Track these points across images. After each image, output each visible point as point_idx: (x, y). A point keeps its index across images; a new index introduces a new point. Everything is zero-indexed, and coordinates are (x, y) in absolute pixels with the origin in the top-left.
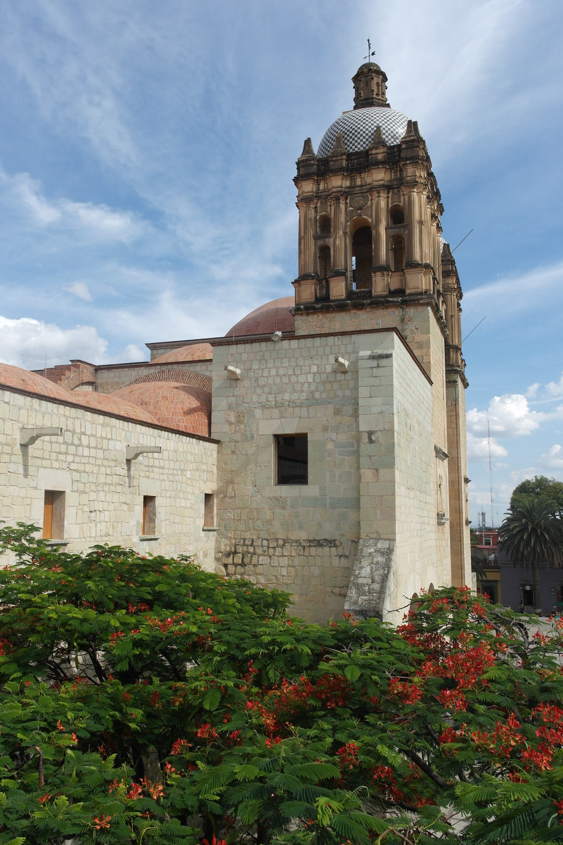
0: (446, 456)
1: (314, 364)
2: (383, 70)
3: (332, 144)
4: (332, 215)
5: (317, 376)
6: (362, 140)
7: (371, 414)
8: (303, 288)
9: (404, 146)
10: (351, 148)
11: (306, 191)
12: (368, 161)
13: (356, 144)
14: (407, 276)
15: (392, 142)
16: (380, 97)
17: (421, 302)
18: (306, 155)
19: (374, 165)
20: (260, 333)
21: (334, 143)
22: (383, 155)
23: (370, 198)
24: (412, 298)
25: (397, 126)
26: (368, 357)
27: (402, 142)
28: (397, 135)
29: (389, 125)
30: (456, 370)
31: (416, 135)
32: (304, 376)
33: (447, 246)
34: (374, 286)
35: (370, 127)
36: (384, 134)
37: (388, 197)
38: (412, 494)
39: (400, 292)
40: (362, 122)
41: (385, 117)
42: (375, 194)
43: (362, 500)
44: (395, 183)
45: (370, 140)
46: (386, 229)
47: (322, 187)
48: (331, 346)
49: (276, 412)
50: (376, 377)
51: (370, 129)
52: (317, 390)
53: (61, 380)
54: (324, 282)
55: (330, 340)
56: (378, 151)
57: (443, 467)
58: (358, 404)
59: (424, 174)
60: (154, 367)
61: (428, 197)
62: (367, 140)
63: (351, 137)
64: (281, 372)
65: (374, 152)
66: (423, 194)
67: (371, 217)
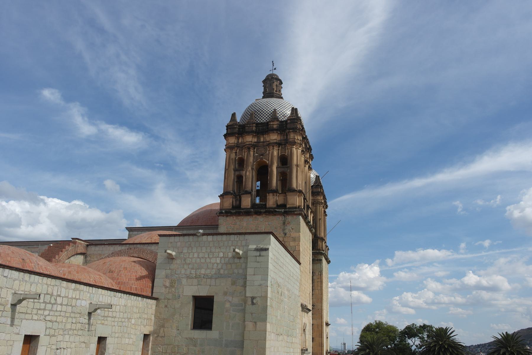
0: (310, 310)
1: (221, 252)
2: (280, 78)
3: (248, 117)
4: (246, 158)
5: (223, 259)
6: (265, 116)
7: (254, 286)
8: (225, 199)
9: (289, 122)
10: (259, 120)
11: (231, 142)
12: (268, 128)
13: (262, 118)
14: (288, 197)
15: (283, 119)
16: (278, 93)
17: (295, 213)
18: (232, 122)
19: (271, 131)
20: (200, 224)
21: (249, 117)
22: (277, 125)
23: (268, 149)
24: (290, 210)
25: (285, 110)
26: (254, 250)
27: (288, 119)
28: (286, 115)
29: (281, 109)
30: (322, 252)
31: (296, 116)
32: (215, 259)
33: (317, 178)
34: (268, 202)
35: (270, 109)
36: (278, 114)
37: (279, 150)
38: (281, 338)
39: (284, 206)
40: (266, 106)
41: (279, 104)
42: (271, 148)
43: (246, 343)
44: (283, 142)
45: (270, 116)
46: (277, 168)
47: (240, 141)
48: (232, 241)
49: (195, 281)
50: (258, 262)
51: (270, 110)
52: (222, 268)
53: (62, 251)
54: (238, 197)
55: (232, 237)
56: (274, 123)
57: (308, 319)
58: (246, 279)
59: (300, 138)
60: (125, 245)
61: (302, 151)
62: (268, 116)
63: (259, 114)
64: (201, 255)
65: (271, 123)
66: (299, 149)
67: (268, 160)
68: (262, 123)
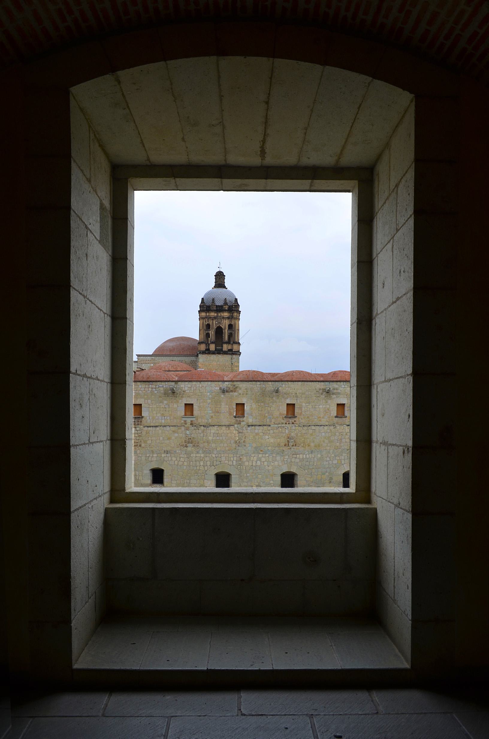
4: (211, 324)
9: (234, 306)
12: (222, 309)
23: (223, 320)
24: (235, 353)
39: (231, 350)
47: (207, 314)
56: (226, 307)
65: (224, 307)
67: (223, 326)
68: (218, 306)
